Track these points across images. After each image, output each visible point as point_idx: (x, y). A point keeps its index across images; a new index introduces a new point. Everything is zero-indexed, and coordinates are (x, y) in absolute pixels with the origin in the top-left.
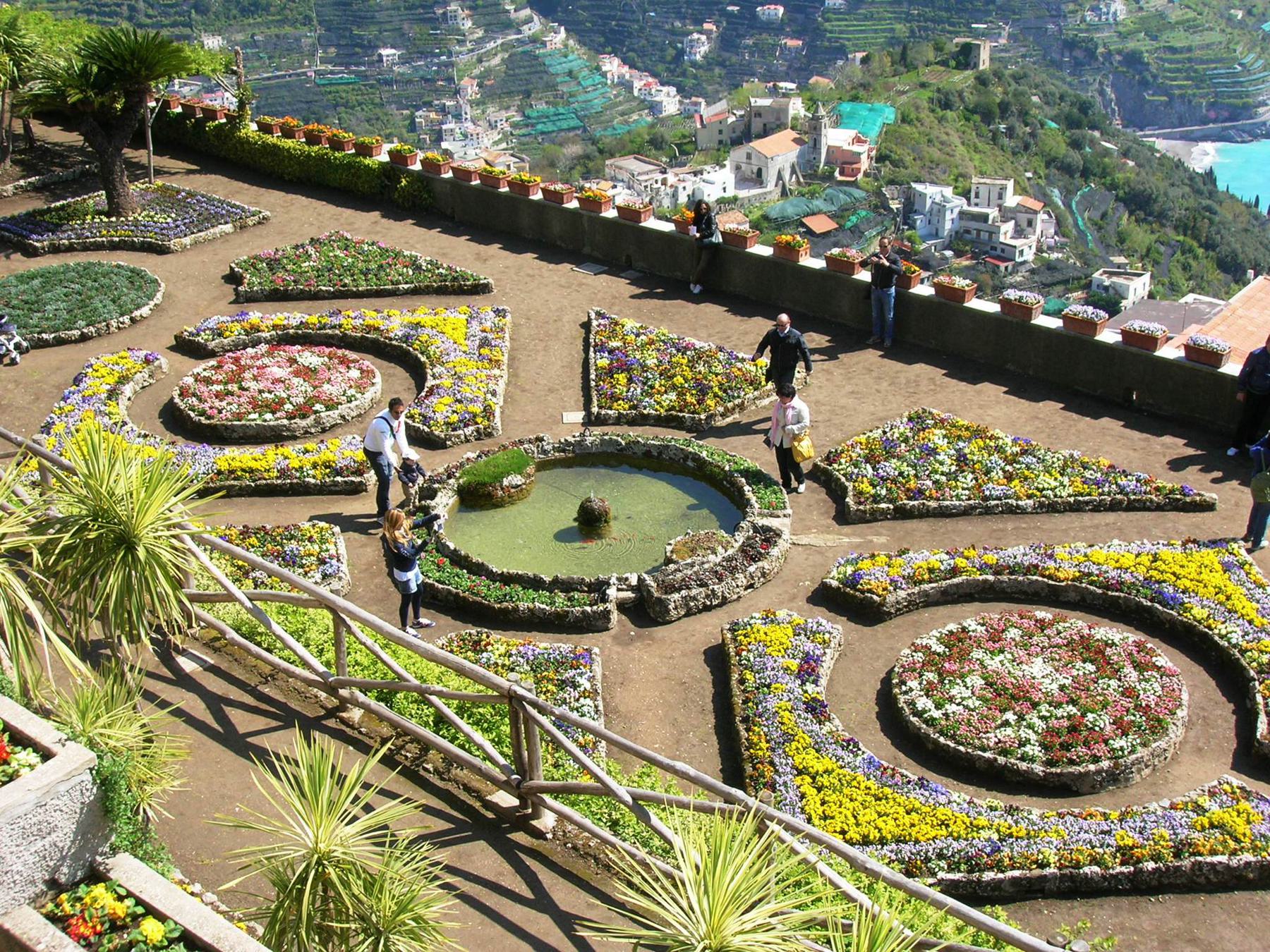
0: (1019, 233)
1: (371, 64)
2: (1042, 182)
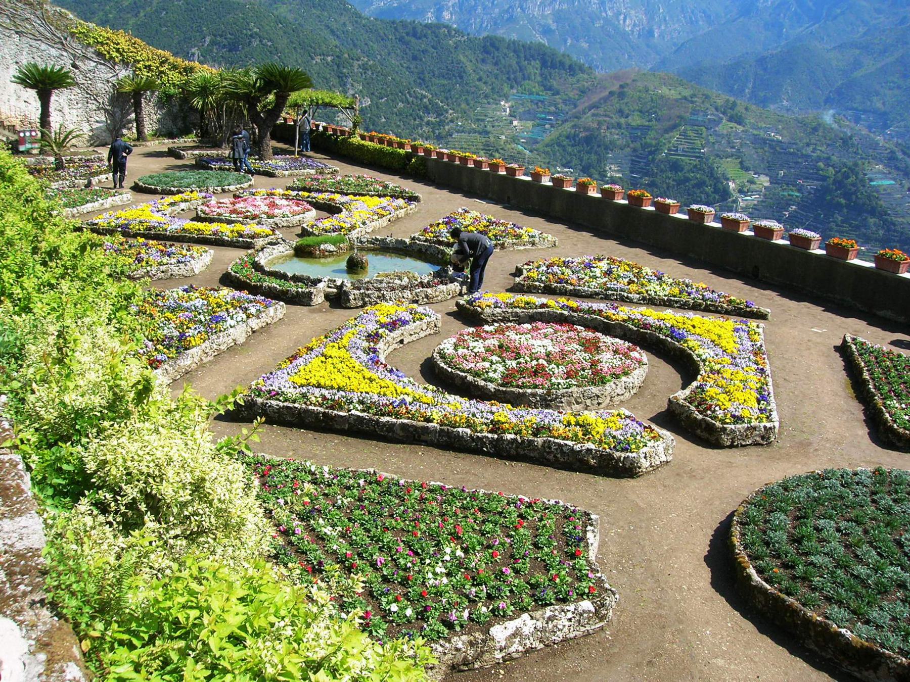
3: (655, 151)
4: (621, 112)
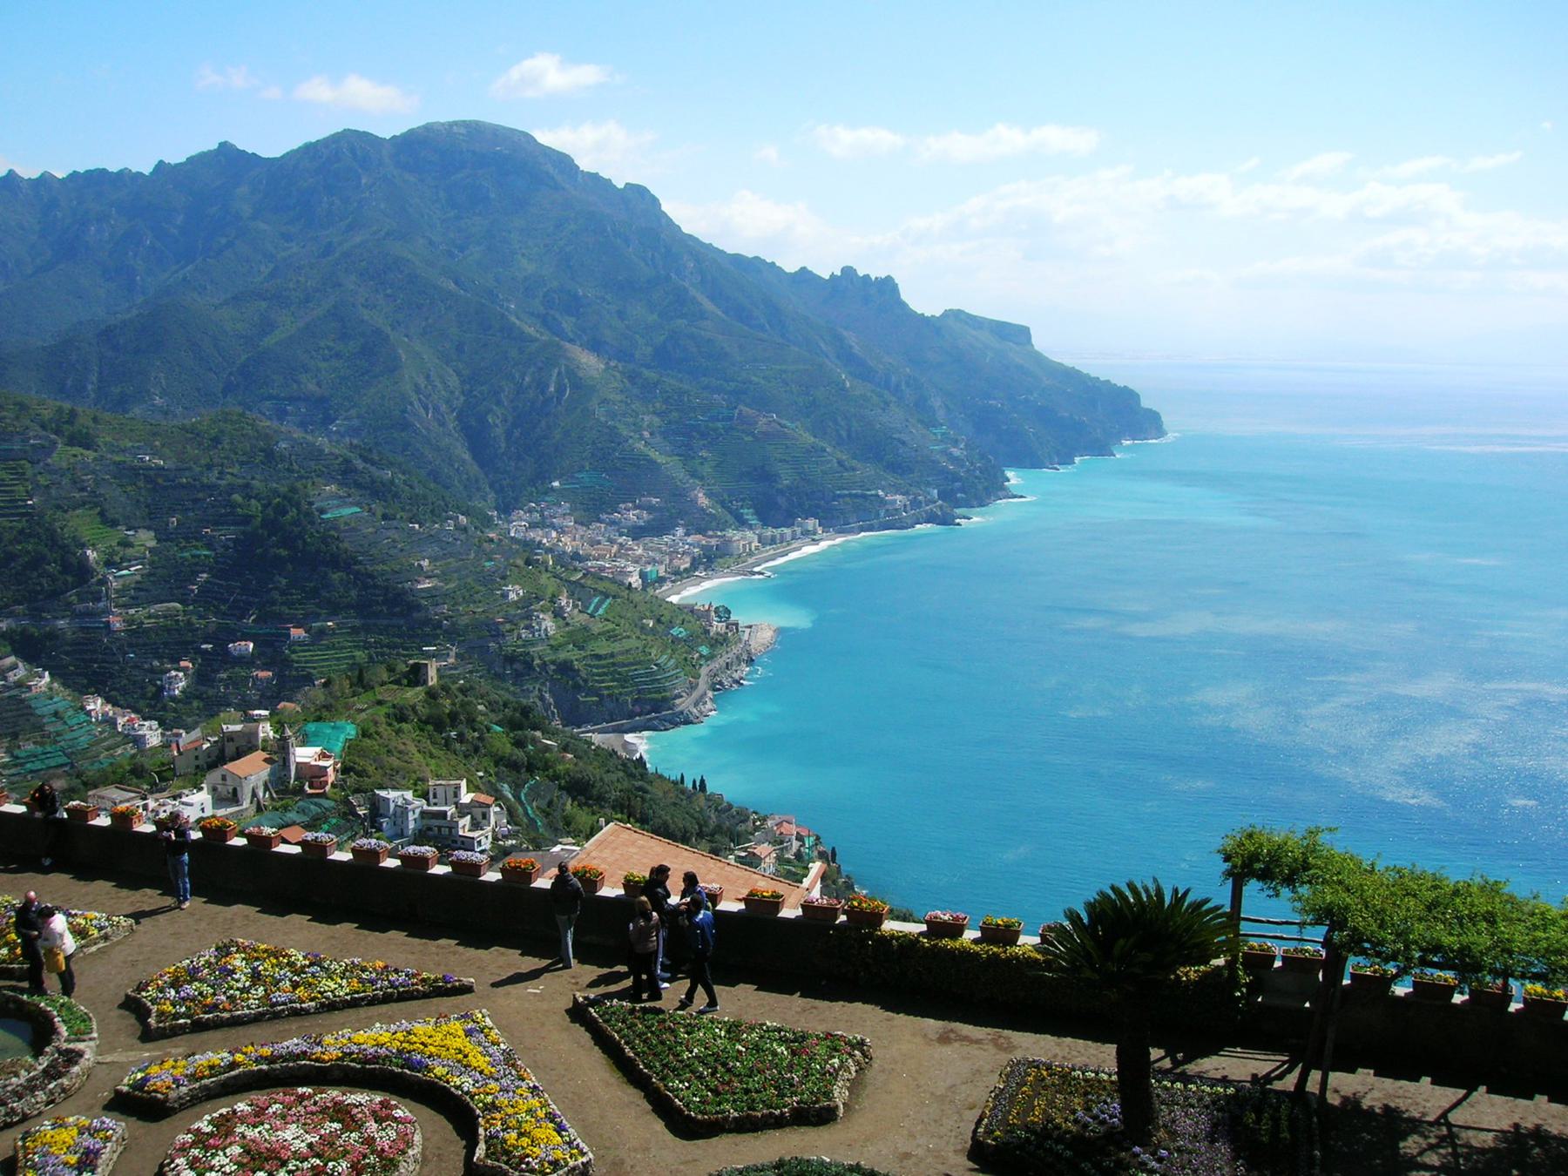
0: (475, 826)
2: (493, 779)
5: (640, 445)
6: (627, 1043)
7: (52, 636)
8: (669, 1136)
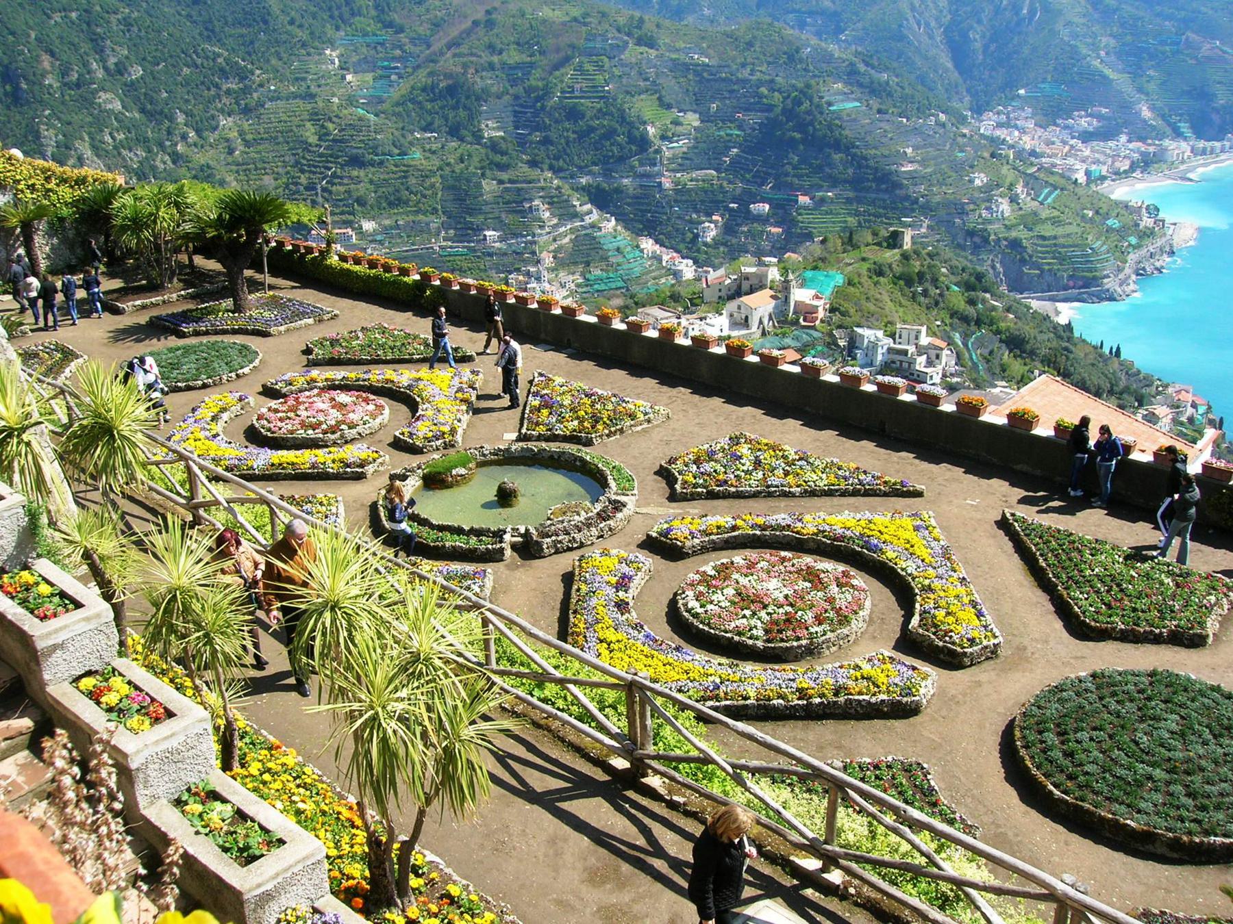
0: (930, 363)
1: (478, 241)
2: (948, 328)
3: (545, 95)
4: (491, 48)
5: (1097, 63)
6: (1041, 555)
7: (618, 191)
8: (1065, 634)
